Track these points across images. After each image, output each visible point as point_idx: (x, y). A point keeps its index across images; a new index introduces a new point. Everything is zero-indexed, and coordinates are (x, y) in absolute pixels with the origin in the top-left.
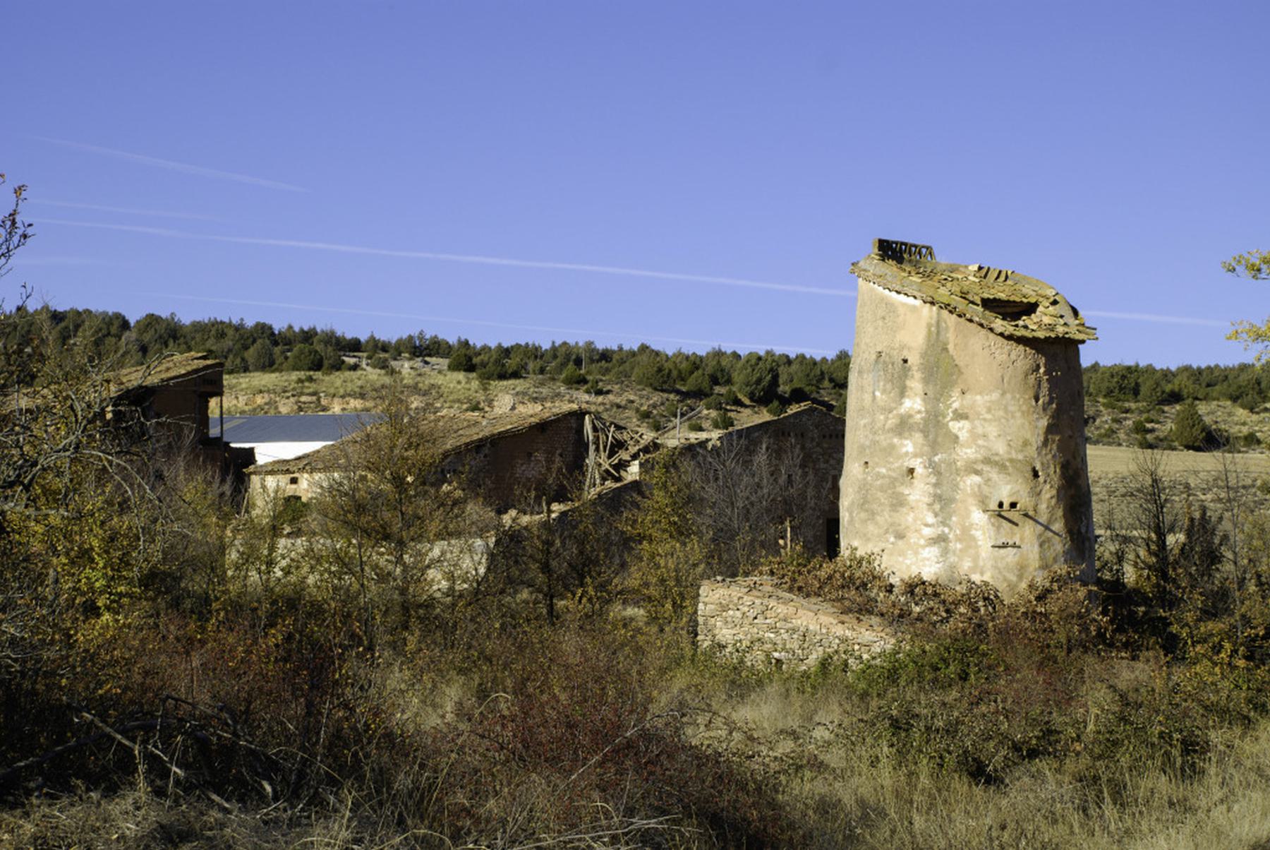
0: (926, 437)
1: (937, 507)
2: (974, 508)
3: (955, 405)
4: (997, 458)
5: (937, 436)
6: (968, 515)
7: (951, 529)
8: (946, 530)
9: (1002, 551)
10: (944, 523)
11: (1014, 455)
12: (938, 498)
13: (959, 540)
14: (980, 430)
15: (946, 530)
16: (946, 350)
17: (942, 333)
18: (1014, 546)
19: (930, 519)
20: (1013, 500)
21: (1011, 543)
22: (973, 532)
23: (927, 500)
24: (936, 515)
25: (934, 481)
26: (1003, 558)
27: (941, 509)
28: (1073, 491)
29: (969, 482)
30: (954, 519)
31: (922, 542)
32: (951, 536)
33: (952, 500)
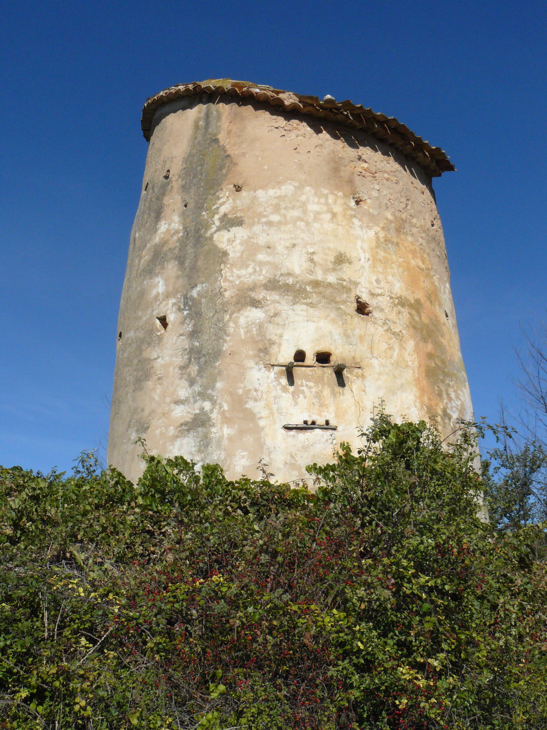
0: (181, 264)
1: (194, 369)
2: (251, 363)
3: (223, 210)
4: (290, 281)
5: (196, 258)
6: (242, 376)
7: (214, 403)
8: (207, 405)
9: (308, 434)
10: (203, 395)
11: (319, 276)
12: (194, 354)
13: (227, 420)
14: (262, 240)
15: (207, 405)
16: (216, 141)
17: (213, 122)
18: (327, 426)
19: (183, 392)
20: (323, 347)
21: (321, 421)
22: (250, 405)
23: (179, 361)
24: (192, 383)
25: (190, 328)
26: (305, 448)
27: (200, 372)
28: (430, 347)
29: (242, 321)
30: (219, 385)
31: (172, 431)
32: (214, 416)
33: (217, 354)
